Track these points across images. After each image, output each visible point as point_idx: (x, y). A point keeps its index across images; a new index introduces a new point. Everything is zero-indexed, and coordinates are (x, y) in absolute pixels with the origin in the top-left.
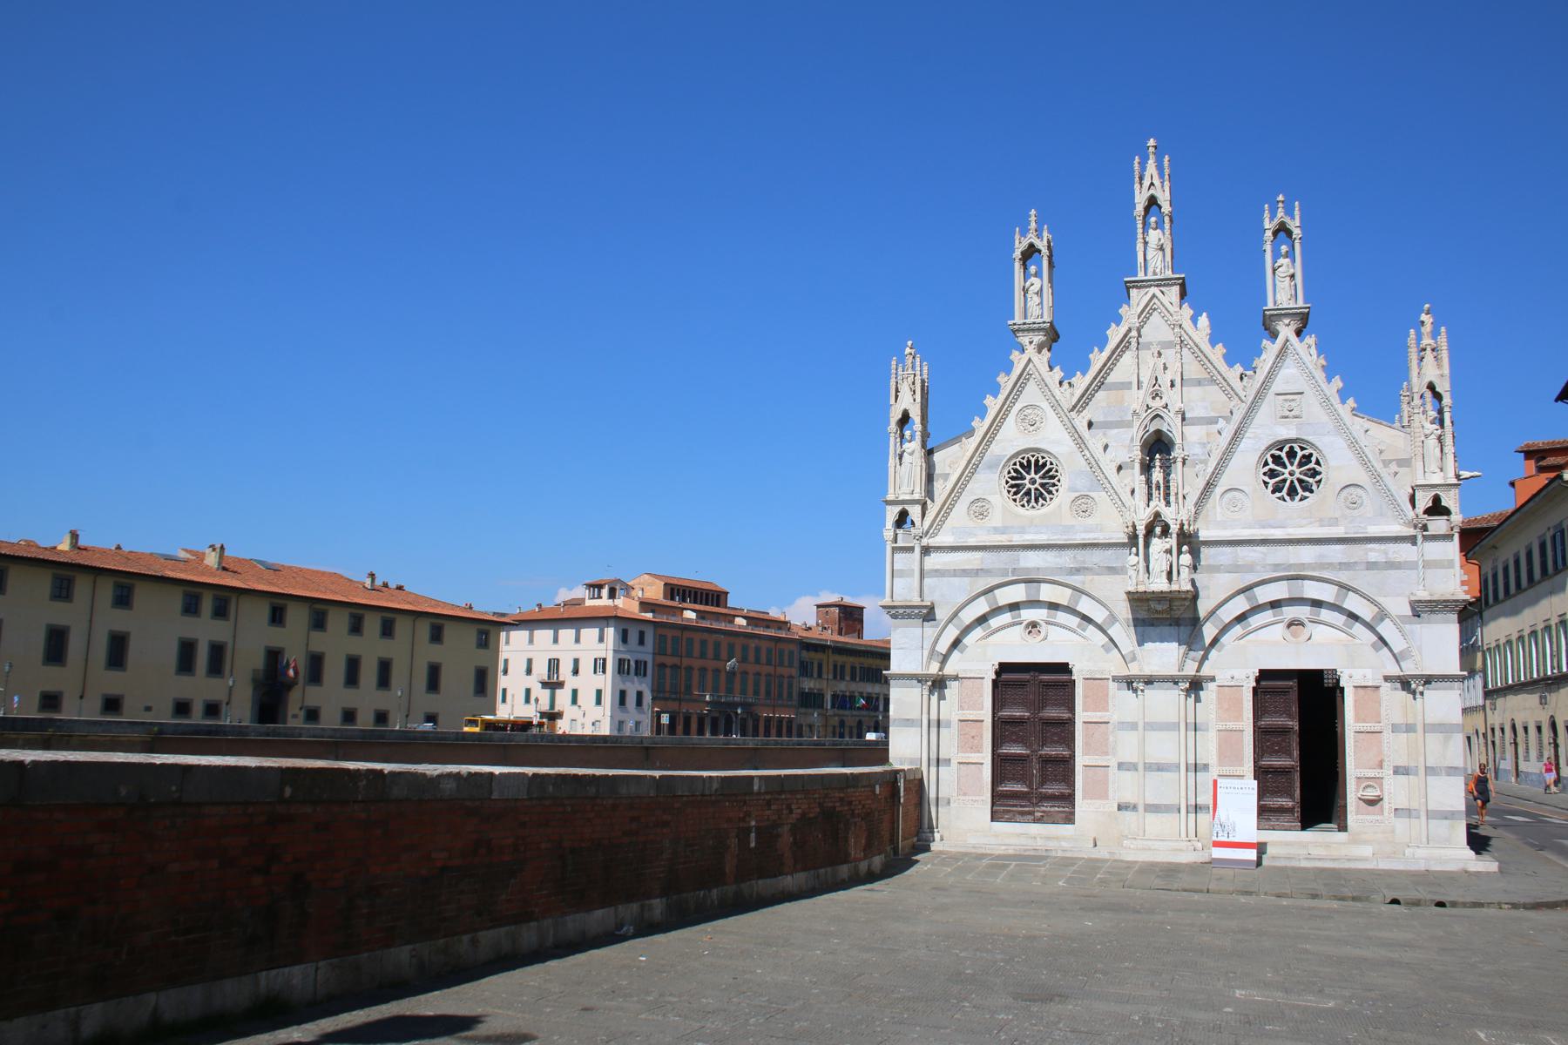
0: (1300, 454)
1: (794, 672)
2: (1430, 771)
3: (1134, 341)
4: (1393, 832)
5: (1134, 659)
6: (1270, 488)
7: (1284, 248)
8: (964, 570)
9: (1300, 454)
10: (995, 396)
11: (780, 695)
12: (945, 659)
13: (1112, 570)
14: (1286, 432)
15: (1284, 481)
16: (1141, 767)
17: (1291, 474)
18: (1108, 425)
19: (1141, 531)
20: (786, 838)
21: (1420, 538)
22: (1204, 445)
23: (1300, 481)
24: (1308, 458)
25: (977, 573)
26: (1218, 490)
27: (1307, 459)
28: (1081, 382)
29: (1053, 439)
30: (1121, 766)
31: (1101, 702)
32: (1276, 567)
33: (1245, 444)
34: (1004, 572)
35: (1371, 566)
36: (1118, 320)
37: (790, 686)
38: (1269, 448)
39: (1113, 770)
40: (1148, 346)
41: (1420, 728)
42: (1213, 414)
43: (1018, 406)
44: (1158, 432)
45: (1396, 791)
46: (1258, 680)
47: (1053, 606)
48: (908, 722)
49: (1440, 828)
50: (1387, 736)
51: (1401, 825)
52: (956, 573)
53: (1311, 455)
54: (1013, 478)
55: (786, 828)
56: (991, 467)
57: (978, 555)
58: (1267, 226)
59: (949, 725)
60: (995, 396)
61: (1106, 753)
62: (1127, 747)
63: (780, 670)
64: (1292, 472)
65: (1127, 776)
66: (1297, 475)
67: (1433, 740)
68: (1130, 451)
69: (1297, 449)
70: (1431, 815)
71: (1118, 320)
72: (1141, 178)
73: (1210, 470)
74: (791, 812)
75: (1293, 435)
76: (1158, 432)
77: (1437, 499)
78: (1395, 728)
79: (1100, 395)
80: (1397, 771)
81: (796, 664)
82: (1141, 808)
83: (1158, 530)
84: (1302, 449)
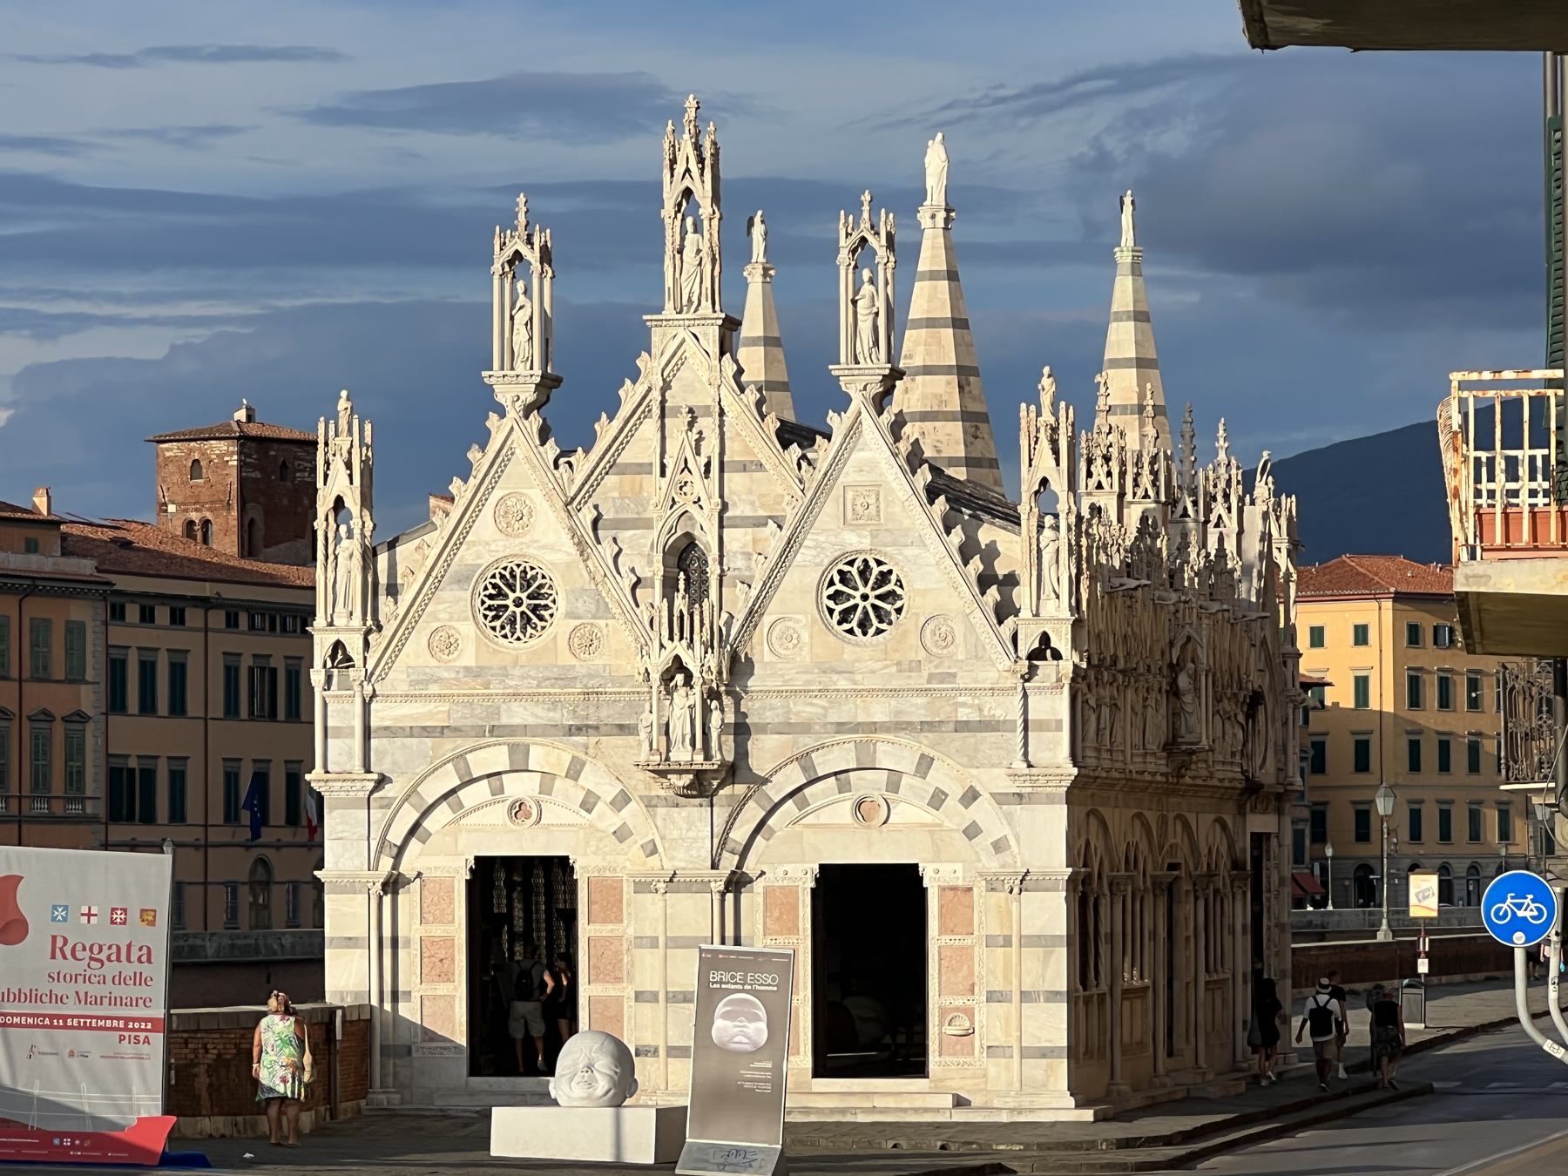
0: (876, 570)
1: (90, 698)
2: (1025, 996)
3: (656, 411)
4: (985, 1076)
5: (654, 851)
6: (836, 616)
7: (866, 274)
8: (424, 728)
9: (876, 570)
10: (465, 481)
11: (41, 781)
12: (401, 849)
13: (623, 729)
14: (857, 542)
15: (856, 607)
16: (662, 996)
17: (865, 597)
18: (620, 524)
19: (655, 677)
20: (203, 1081)
21: (1020, 688)
22: (748, 556)
23: (874, 606)
24: (884, 578)
25: (442, 731)
26: (767, 620)
27: (884, 578)
28: (583, 463)
29: (548, 544)
30: (639, 996)
31: (612, 909)
32: (840, 727)
33: (803, 556)
34: (479, 732)
35: (962, 727)
36: (635, 376)
37: (75, 751)
38: (834, 562)
39: (629, 1005)
40: (677, 411)
41: (1015, 941)
42: (762, 513)
43: (497, 494)
44: (687, 534)
45: (991, 1023)
46: (817, 880)
47: (548, 779)
48: (351, 942)
49: (1036, 1068)
50: (980, 952)
51: (994, 1067)
52: (412, 732)
53: (890, 572)
54: (491, 597)
55: (202, 1069)
56: (462, 580)
57: (444, 707)
58: (842, 242)
59: (408, 942)
60: (465, 481)
61: (619, 980)
62: (647, 970)
63: (40, 696)
64: (861, 596)
65: (647, 1008)
66: (872, 600)
67: (1031, 956)
68: (650, 563)
69: (873, 564)
70: (1025, 1053)
71: (635, 376)
72: (673, 162)
73: (754, 593)
74: (207, 1051)
75: (866, 543)
76: (687, 534)
77: (1045, 639)
78: (990, 942)
79: (611, 480)
80: (992, 997)
81: (95, 668)
82: (662, 1052)
83: (679, 678)
84: (879, 563)
